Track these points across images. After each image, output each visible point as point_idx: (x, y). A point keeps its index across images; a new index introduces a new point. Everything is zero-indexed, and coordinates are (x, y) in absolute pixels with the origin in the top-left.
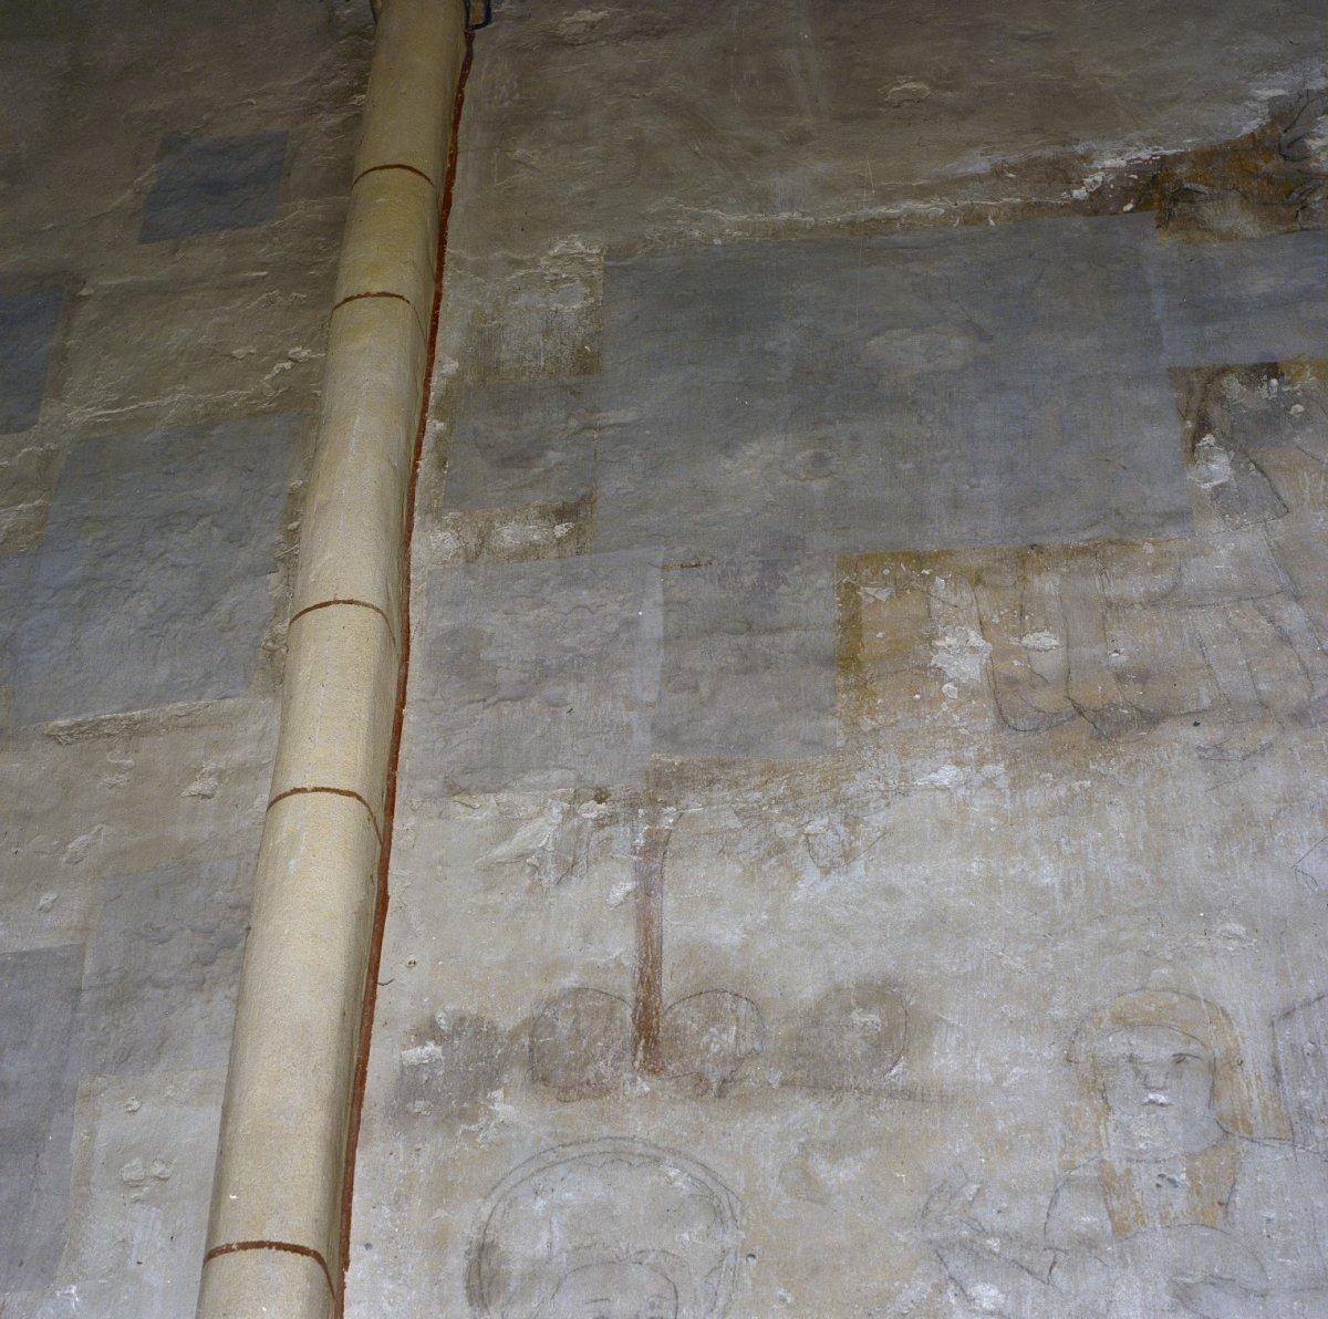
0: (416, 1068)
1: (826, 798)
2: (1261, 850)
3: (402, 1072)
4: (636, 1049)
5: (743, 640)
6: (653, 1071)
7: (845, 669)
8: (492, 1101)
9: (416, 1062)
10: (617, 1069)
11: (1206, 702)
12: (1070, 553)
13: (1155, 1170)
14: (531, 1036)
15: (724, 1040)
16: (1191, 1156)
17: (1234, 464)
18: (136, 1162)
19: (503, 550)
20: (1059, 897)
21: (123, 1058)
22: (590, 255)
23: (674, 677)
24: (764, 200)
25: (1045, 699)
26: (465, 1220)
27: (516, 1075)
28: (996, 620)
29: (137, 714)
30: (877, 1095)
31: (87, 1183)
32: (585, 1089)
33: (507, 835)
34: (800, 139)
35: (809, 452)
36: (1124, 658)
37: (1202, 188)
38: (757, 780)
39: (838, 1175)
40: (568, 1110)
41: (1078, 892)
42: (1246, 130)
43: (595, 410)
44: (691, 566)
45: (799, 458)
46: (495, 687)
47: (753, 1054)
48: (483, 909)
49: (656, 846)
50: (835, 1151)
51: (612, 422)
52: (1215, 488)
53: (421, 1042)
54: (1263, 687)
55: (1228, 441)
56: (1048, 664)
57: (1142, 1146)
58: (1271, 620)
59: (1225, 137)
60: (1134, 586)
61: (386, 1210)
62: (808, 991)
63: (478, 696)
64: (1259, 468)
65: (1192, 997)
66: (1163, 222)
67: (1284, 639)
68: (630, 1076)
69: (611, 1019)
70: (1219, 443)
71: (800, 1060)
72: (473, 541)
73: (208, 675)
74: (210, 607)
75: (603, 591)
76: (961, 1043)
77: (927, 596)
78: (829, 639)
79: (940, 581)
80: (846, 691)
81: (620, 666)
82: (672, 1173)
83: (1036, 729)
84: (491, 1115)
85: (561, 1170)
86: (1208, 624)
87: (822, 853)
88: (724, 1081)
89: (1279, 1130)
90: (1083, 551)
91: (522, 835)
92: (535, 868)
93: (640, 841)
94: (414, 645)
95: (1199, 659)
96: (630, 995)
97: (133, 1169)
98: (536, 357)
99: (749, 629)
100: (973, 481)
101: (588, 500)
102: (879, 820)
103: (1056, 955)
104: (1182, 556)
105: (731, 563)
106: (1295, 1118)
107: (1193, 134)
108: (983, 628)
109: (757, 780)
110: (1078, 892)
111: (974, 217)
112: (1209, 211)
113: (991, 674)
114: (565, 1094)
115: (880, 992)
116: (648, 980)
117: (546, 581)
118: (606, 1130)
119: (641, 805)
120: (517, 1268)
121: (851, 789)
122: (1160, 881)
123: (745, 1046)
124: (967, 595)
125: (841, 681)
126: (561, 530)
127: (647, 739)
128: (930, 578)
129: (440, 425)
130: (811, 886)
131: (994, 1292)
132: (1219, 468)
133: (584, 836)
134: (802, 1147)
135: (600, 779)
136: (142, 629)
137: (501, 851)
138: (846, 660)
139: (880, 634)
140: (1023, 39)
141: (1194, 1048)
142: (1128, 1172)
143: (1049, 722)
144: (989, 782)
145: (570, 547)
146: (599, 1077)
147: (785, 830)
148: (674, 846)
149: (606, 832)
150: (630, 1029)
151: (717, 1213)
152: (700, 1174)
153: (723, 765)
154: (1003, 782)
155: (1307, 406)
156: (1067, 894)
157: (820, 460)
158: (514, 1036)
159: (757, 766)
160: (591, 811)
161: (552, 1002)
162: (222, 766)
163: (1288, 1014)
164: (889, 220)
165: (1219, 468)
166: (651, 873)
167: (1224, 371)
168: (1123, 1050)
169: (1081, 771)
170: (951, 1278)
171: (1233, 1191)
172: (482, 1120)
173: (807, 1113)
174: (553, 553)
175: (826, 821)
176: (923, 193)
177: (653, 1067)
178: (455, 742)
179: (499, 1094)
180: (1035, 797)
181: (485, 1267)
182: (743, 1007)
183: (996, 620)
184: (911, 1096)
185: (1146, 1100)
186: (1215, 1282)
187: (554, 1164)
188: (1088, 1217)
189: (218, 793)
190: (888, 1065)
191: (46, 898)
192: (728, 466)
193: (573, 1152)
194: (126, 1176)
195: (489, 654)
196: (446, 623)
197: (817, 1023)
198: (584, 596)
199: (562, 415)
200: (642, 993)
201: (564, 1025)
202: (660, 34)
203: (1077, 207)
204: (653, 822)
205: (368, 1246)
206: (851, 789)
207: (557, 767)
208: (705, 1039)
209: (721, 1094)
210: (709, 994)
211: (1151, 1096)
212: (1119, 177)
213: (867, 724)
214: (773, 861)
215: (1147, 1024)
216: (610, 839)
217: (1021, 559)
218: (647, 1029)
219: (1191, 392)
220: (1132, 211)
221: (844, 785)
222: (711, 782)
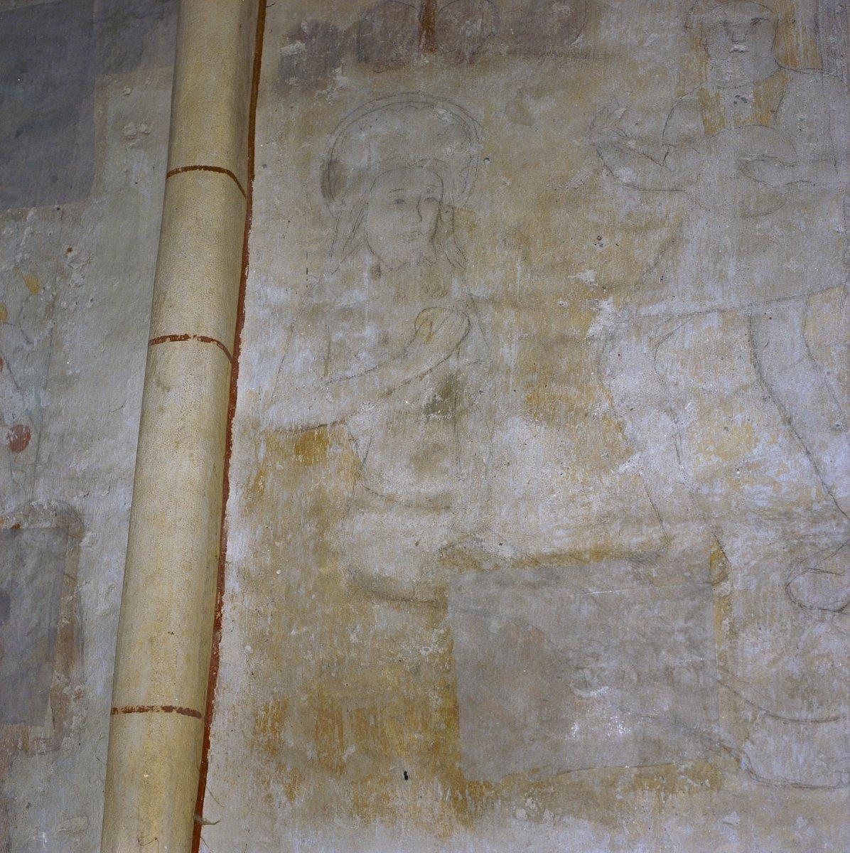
0: (291, 57)
3: (282, 61)
4: (421, 37)
8: (335, 75)
9: (290, 54)
10: (409, 50)
14: (358, 33)
16: (757, 84)
27: (349, 58)
47: (492, 35)
50: (539, 93)
53: (292, 41)
57: (727, 78)
68: (417, 54)
88: (473, 54)
89: (813, 63)
106: (825, 56)
118: (403, 89)
131: (630, 172)
134: (519, 92)
141: (765, 14)
142: (717, 95)
146: (398, 55)
152: (457, 111)
158: (347, 34)
168: (720, 18)
170: (605, 165)
171: (781, 103)
172: (330, 87)
177: (431, 48)
179: (339, 70)
181: (332, 174)
184: (586, 56)
185: (732, 49)
186: (763, 159)
188: (690, 124)
201: (378, 26)
205: (265, 166)
209: (471, 62)
211: (736, 47)
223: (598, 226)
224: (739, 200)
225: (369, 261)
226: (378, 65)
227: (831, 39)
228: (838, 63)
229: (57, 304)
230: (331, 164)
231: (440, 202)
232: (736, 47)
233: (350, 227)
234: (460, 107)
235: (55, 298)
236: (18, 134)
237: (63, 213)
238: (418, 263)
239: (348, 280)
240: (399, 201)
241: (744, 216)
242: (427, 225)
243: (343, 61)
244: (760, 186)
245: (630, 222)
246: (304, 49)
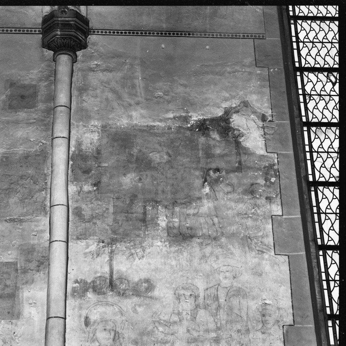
0: (75, 287)
1: (140, 246)
2: (206, 262)
5: (126, 215)
7: (144, 222)
8: (87, 294)
11: (201, 235)
12: (182, 204)
13: (186, 312)
15: (123, 287)
16: (191, 310)
17: (210, 189)
18: (31, 300)
20: (175, 266)
21: (27, 282)
23: (115, 221)
24: (131, 117)
25: (175, 231)
26: (84, 313)
27: (91, 290)
28: (169, 215)
29: (21, 218)
30: (146, 297)
31: (23, 303)
32: (102, 293)
34: (138, 104)
35: (138, 177)
36: (188, 225)
37: (211, 127)
39: (140, 310)
40: (99, 296)
41: (178, 266)
42: (220, 115)
43: (100, 163)
44: (118, 198)
45: (137, 178)
46: (84, 219)
47: (128, 289)
48: (84, 261)
50: (140, 306)
51: (103, 166)
52: (206, 194)
54: (210, 233)
55: (209, 184)
56: (176, 225)
58: (212, 221)
59: (216, 116)
60: (191, 211)
61: (71, 310)
62: (136, 280)
63: (82, 221)
64: (214, 190)
65: (194, 285)
66: (203, 135)
67: (214, 224)
69: (105, 281)
70: (208, 184)
71: (135, 291)
72: (79, 189)
73: (33, 211)
74: (32, 197)
75: (103, 202)
76: (159, 290)
77: (158, 209)
78: (141, 216)
79: (160, 207)
80: (144, 226)
81: (106, 218)
82: (115, 307)
83: (174, 237)
85: (98, 306)
86: (202, 220)
87: (139, 256)
90: (184, 203)
91: (90, 248)
92: (93, 254)
93: (110, 251)
94: (70, 209)
95: (200, 226)
96: (108, 278)
97: (31, 301)
98: (89, 149)
100: (166, 187)
101: (99, 182)
102: (148, 251)
103: (174, 277)
104: (200, 206)
105: (125, 199)
107: (210, 114)
108: (166, 216)
110: (178, 266)
111: (170, 128)
112: (211, 133)
113: (167, 225)
114: (99, 293)
115: (147, 281)
117: (93, 199)
118: (105, 300)
119: (110, 244)
120: (92, 321)
121: (144, 245)
122: (191, 265)
123: (126, 288)
124: (164, 210)
125: (143, 224)
126: (95, 188)
127: (111, 232)
128: (158, 206)
129: (72, 162)
130: (137, 261)
131: (162, 329)
132: (207, 190)
133: (100, 249)
134: (135, 305)
135: (103, 238)
136: (20, 200)
137: (87, 251)
138: (144, 220)
139: (149, 216)
140: (181, 85)
141: (193, 293)
142: (182, 312)
143: (175, 236)
144: (166, 246)
145: (96, 192)
146: (104, 291)
147: (133, 251)
148: (115, 252)
149: (104, 249)
150: (108, 284)
151: (122, 314)
152: (119, 308)
153: (123, 238)
154: (168, 246)
155: (223, 179)
156: (176, 266)
157: (140, 179)
158: (90, 283)
160: (101, 244)
161: (96, 278)
162: (38, 230)
163: (207, 289)
164: (154, 126)
165: (207, 190)
166: (112, 257)
167: (210, 169)
169: (180, 245)
171: (197, 316)
172: (86, 297)
173: (135, 299)
174: (94, 193)
175: (139, 250)
176: (161, 121)
177: (112, 290)
178: (78, 229)
179: (88, 293)
180: (173, 249)
181: (87, 320)
182: (126, 281)
183: (169, 215)
184: (151, 298)
187: (97, 305)
189: (38, 235)
190: (148, 293)
191: (9, 252)
192: (124, 178)
193: (100, 303)
195: (83, 213)
196: (75, 206)
197: (137, 285)
198: (100, 203)
199: (94, 163)
202: (111, 71)
203: (188, 128)
204: (112, 247)
205: (69, 316)
206: (144, 245)
207: (96, 236)
208: (120, 286)
209: (123, 295)
210: (120, 278)
211: (186, 300)
212: (196, 123)
213: (147, 233)
214: (131, 257)
215: (187, 289)
217: (174, 204)
218: (112, 285)
219: (204, 173)
220: (198, 131)
221: (143, 244)
222: (121, 241)
223: (154, 341)
224: (187, 338)
226: (99, 293)
227: (208, 302)
228: (209, 308)
230: (87, 318)
231: (115, 331)
232: (186, 300)
233: (92, 335)
234: (120, 307)
237: (12, 322)
240: (105, 330)
241: (188, 342)
242: (112, 336)
243: (89, 290)
244: (192, 335)
245: (162, 341)
246: (78, 286)
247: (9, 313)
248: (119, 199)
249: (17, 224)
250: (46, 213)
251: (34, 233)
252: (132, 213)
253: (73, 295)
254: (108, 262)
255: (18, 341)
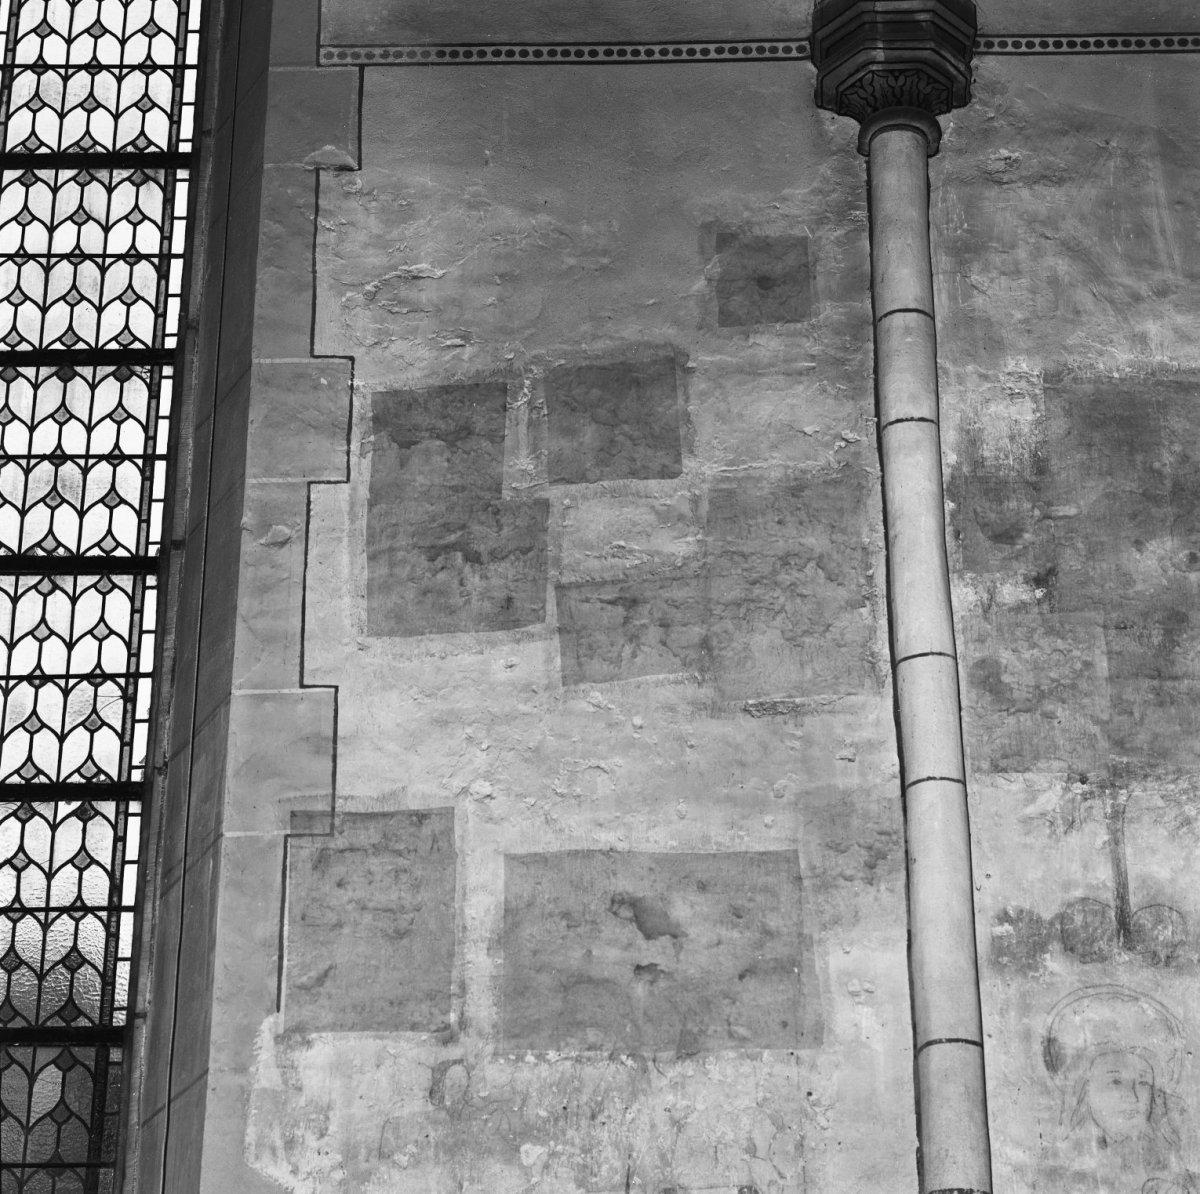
5: (1156, 683)
6: (1129, 949)
8: (1044, 960)
14: (1061, 923)
15: (1165, 934)
19: (1005, 604)
22: (1032, 376)
23: (1119, 705)
24: (1142, 339)
26: (1039, 1025)
27: (1055, 946)
31: (830, 992)
33: (1032, 799)
34: (1162, 292)
35: (1187, 552)
38: (1171, 777)
40: (1087, 967)
43: (1049, 504)
44: (1121, 627)
46: (1013, 702)
47: (1182, 943)
49: (1117, 814)
51: (1061, 514)
61: (997, 1017)
63: (1004, 707)
84: (1045, 967)
85: (1086, 1002)
91: (1042, 799)
92: (1052, 823)
96: (1112, 904)
97: (855, 986)
98: (1007, 457)
99: (1159, 675)
109: (1171, 777)
114: (1085, 958)
116: (1122, 896)
118: (1108, 981)
120: (1069, 1052)
123: (1177, 938)
126: (1039, 593)
137: (1031, 810)
145: (1046, 607)
148: (1128, 815)
149: (1088, 803)
150: (1115, 923)
151: (1170, 1029)
152: (1159, 1007)
158: (1051, 923)
159: (1171, 768)
160: (1078, 788)
161: (1070, 905)
166: (1118, 830)
172: (1041, 971)
177: (1129, 946)
179: (1048, 956)
182: (1175, 915)
191: (768, 819)
194: (851, 989)
195: (1006, 678)
199: (1029, 506)
200: (1119, 902)
202: (1060, 182)
204: (1114, 797)
208: (1156, 932)
209: (1167, 964)
214: (1185, 829)
216: (1091, 807)
222: (1146, 776)
225: (1095, 1132)
229: (805, 1143)
230: (1050, 1042)
231: (1152, 1087)
234: (1162, 1005)
235: (803, 1138)
236: (741, 977)
238: (1139, 1139)
239: (1079, 1147)
240: (1116, 1082)
242: (1143, 1105)
243: (1050, 948)
246: (1012, 931)
247: (785, 1024)
248: (1125, 628)
249: (785, 723)
250: (881, 684)
251: (847, 753)
252: (1175, 678)
253: (998, 966)
254: (1108, 850)
255: (824, 1123)
